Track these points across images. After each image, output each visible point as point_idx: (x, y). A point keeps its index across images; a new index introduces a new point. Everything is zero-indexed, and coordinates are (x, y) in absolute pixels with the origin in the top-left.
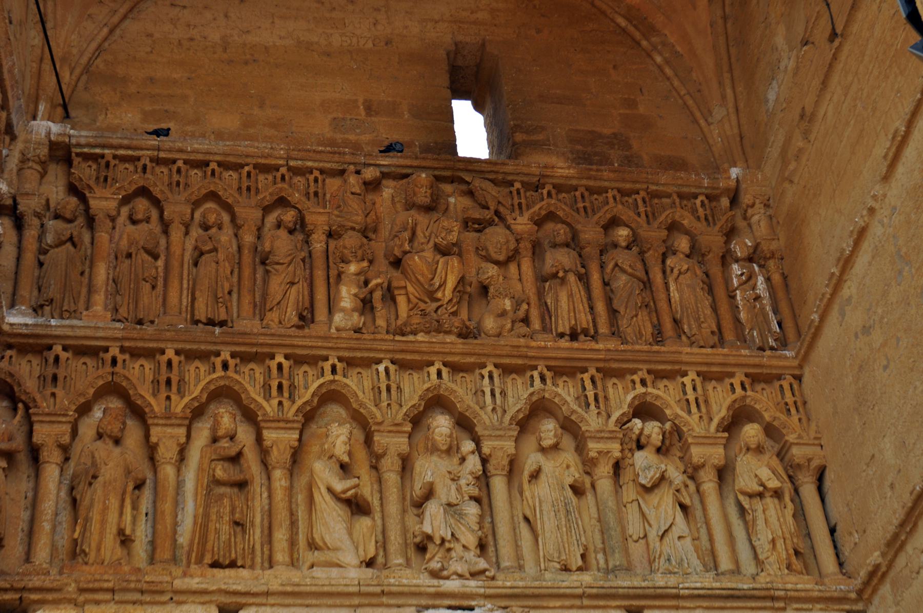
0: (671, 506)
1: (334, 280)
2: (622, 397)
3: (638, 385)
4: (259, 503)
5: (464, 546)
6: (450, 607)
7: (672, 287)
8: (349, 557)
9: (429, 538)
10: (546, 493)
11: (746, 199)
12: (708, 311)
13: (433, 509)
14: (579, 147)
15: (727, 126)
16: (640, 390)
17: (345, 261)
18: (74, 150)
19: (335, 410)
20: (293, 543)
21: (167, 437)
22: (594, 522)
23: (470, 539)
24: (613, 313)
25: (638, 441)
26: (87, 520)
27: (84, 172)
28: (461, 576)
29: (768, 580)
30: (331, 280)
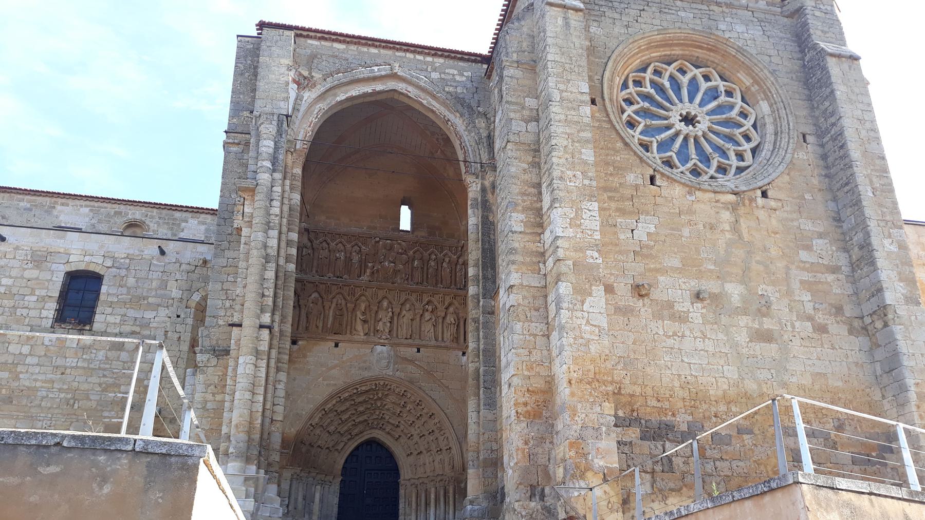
1: (366, 267)
2: (426, 299)
4: (345, 319)
8: (362, 334)
10: (405, 321)
13: (381, 323)
19: (363, 298)
21: (327, 304)
23: (387, 331)
27: (312, 236)
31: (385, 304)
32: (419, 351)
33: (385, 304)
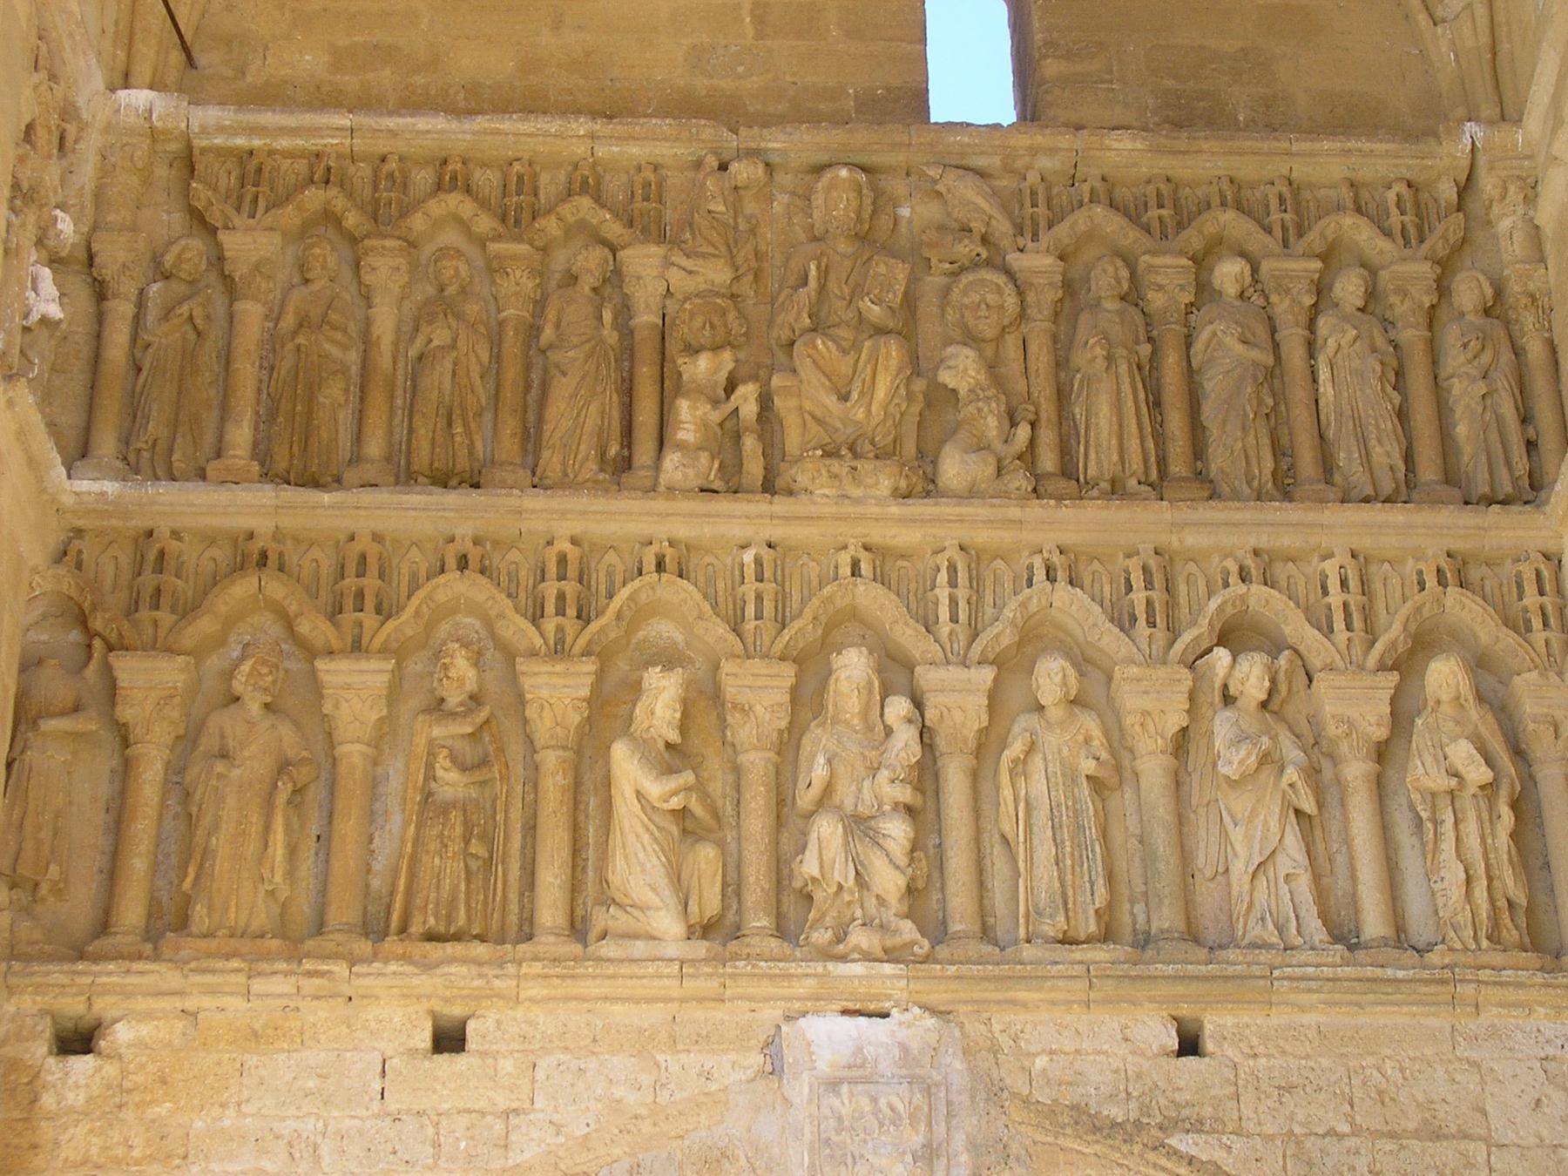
0: (1277, 817)
3: (1234, 579)
5: (878, 897)
6: (845, 1012)
7: (1324, 374)
8: (668, 923)
9: (814, 880)
11: (1488, 184)
12: (1389, 424)
14: (1169, 83)
15: (1467, 30)
16: (1238, 588)
17: (693, 350)
18: (196, 142)
20: (575, 888)
22: (1133, 843)
24: (1196, 429)
25: (1225, 686)
26: (206, 853)
28: (868, 957)
29: (1447, 961)
30: (667, 384)
31: (853, 668)
32: (1189, 1045)
33: (853, 668)
